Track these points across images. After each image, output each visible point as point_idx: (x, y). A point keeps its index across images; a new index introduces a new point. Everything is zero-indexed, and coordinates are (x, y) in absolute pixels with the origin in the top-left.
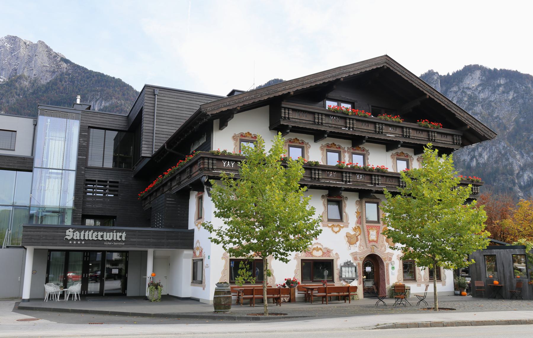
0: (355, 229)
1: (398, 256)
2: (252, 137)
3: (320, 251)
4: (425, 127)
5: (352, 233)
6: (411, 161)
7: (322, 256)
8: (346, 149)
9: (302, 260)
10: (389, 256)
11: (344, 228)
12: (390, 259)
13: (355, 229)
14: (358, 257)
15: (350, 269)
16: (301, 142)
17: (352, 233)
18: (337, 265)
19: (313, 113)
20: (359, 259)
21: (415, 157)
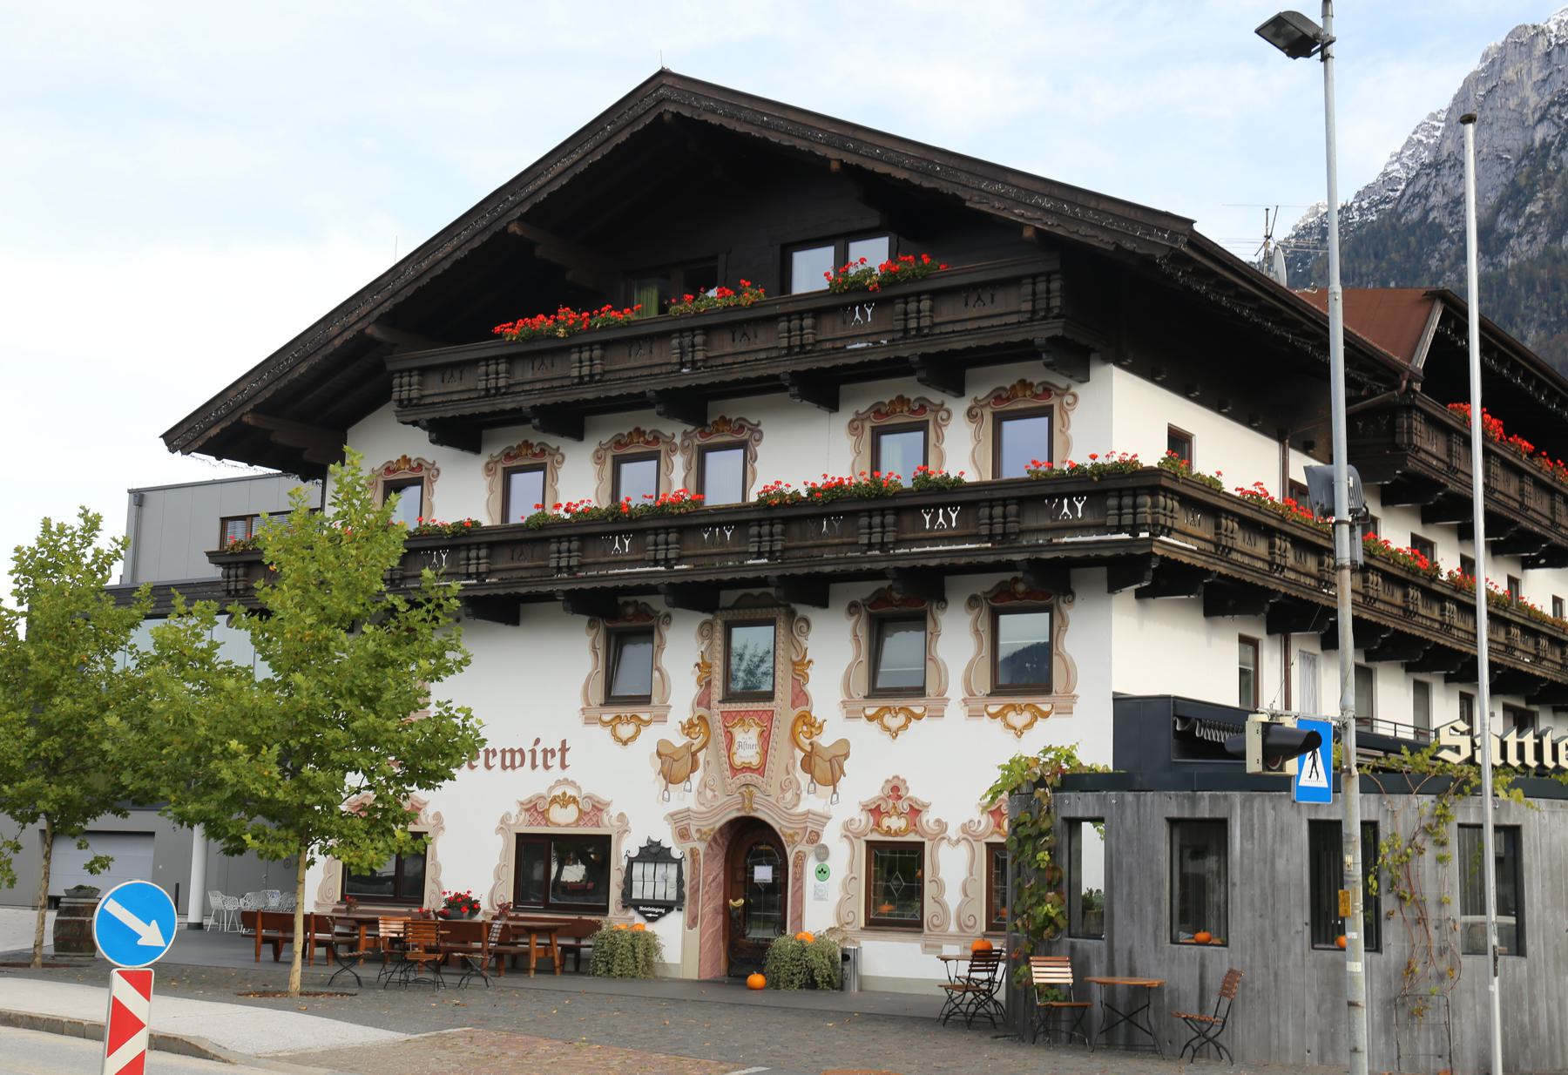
0: (691, 725)
1: (847, 826)
2: (412, 469)
3: (572, 809)
4: (857, 290)
5: (679, 741)
6: (938, 426)
7: (577, 823)
8: (678, 440)
9: (519, 836)
10: (811, 827)
11: (653, 726)
12: (815, 837)
13: (688, 728)
14: (693, 830)
15: (661, 869)
16: (537, 450)
17: (679, 741)
18: (619, 852)
19: (474, 363)
20: (696, 836)
21: (958, 408)
